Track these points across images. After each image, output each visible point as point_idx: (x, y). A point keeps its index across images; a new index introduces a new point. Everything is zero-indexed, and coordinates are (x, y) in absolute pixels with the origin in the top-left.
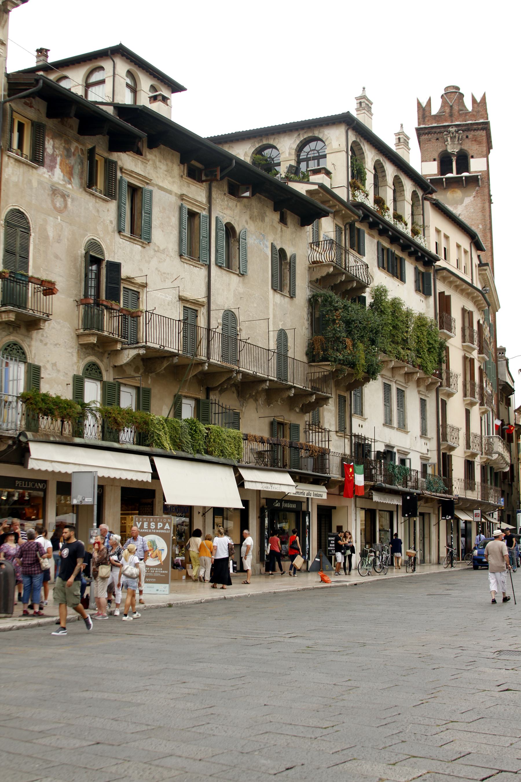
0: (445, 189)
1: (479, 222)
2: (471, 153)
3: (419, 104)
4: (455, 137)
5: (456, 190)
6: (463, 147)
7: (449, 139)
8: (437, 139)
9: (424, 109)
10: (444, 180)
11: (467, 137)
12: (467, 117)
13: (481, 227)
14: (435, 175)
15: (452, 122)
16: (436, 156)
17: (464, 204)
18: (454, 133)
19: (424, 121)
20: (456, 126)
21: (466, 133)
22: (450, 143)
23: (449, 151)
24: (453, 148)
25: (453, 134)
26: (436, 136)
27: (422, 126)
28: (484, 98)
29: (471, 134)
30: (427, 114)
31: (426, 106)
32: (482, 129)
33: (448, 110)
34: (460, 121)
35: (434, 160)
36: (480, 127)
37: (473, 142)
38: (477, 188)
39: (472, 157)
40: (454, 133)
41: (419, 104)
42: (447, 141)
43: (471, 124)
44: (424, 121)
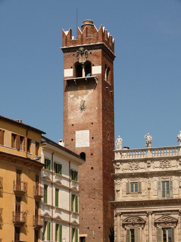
0: (77, 86)
1: (96, 105)
2: (93, 63)
5: (83, 86)
6: (88, 59)
8: (74, 55)
9: (66, 37)
10: (75, 80)
11: (91, 53)
12: (91, 41)
13: (97, 108)
14: (71, 77)
15: (82, 44)
16: (72, 65)
19: (66, 44)
20: (83, 46)
21: (90, 51)
22: (80, 57)
23: (80, 62)
24: (82, 60)
26: (73, 53)
27: (65, 47)
29: (93, 51)
30: (69, 39)
32: (100, 48)
33: (80, 37)
34: (87, 44)
35: (72, 68)
37: (94, 56)
39: (93, 65)
41: (64, 34)
44: (66, 44)
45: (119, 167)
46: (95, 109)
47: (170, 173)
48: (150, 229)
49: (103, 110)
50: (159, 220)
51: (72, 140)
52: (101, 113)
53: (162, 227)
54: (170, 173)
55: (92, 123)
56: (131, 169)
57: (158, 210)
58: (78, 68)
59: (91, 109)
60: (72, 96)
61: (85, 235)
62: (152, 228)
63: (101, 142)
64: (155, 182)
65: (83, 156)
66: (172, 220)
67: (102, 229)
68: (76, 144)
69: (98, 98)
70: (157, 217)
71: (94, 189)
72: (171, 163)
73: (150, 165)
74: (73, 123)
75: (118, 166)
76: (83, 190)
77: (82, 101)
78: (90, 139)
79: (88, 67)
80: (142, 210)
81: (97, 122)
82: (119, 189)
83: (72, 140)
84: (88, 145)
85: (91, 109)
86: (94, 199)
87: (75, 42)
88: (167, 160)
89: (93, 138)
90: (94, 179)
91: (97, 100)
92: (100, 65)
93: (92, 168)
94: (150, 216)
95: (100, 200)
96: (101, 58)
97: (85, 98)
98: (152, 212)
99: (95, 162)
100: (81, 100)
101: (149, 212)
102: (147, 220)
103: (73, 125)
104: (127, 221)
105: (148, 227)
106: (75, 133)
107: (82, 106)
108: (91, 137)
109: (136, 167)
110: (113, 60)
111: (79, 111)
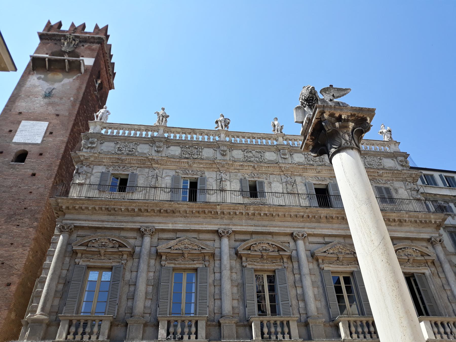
0: (48, 71)
3: (49, 22)
4: (72, 43)
5: (59, 73)
7: (66, 43)
8: (56, 44)
10: (47, 59)
13: (72, 99)
17: (62, 83)
18: (71, 39)
25: (70, 39)
26: (55, 42)
32: (98, 43)
36: (96, 41)
38: (79, 74)
40: (71, 39)
42: (64, 44)
43: (89, 37)
45: (94, 145)
46: (69, 99)
47: (201, 166)
48: (143, 266)
49: (82, 104)
52: (78, 105)
53: (173, 265)
54: (201, 166)
59: (61, 99)
62: (149, 266)
63: (66, 139)
64: (167, 178)
65: (22, 157)
66: (202, 248)
67: (13, 288)
69: (80, 88)
71: (25, 208)
72: (203, 152)
74: (21, 111)
75: (92, 143)
78: (46, 133)
80: (130, 224)
81: (67, 114)
84: (39, 141)
85: (61, 99)
87: (64, 31)
88: (196, 147)
91: (75, 92)
92: (93, 58)
94: (147, 240)
95: (31, 230)
96: (97, 52)
97: (56, 85)
99: (44, 171)
101: (146, 230)
103: (20, 113)
105: (136, 264)
106: (19, 123)
107: (47, 92)
108: (50, 130)
110: (110, 89)
111: (40, 98)
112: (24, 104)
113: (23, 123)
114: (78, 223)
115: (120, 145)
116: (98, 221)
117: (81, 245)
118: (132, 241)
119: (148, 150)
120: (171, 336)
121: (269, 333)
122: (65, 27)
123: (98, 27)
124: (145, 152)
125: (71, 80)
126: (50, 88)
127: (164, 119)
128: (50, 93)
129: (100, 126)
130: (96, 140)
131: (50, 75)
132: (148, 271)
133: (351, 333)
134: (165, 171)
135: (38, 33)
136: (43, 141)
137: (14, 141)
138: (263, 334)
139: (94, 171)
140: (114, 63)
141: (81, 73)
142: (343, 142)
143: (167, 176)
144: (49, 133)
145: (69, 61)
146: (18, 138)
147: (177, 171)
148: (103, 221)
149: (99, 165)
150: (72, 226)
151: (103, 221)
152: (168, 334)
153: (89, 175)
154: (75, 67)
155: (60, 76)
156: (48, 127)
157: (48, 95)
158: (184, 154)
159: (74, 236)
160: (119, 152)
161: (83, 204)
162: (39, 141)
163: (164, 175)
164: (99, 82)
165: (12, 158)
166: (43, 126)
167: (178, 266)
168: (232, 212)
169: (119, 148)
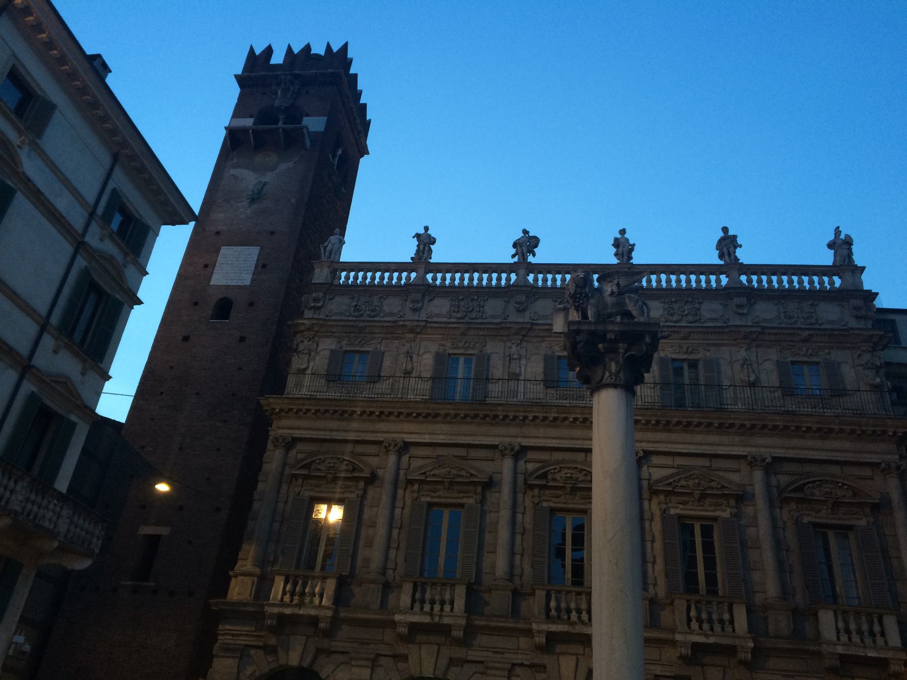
3: (252, 50)
8: (264, 94)
11: (307, 92)
13: (293, 201)
17: (277, 171)
28: (345, 47)
31: (260, 54)
35: (251, 117)
39: (308, 116)
41: (252, 50)
42: (276, 94)
45: (319, 305)
50: (424, 473)
51: (206, 266)
53: (428, 499)
54: (482, 333)
55: (272, 233)
56: (356, 314)
57: (427, 439)
58: (265, 117)
60: (232, 171)
61: (164, 531)
64: (427, 356)
66: (472, 474)
68: (214, 276)
70: (416, 463)
71: (233, 394)
73: (419, 305)
76: (197, 394)
77: (260, 182)
78: (256, 266)
79: (294, 115)
82: (303, 367)
83: (206, 266)
84: (248, 283)
86: (225, 421)
89: (264, 266)
90: (240, 369)
93: (242, 339)
97: (268, 177)
98: (402, 444)
100: (256, 181)
102: (380, 472)
103: (218, 233)
104: (307, 466)
106: (218, 251)
109: (372, 311)
111: (246, 203)
112: (221, 216)
113: (224, 250)
114: (298, 433)
115: (359, 300)
116: (325, 430)
117: (302, 467)
118: (374, 461)
119: (399, 308)
120: (417, 605)
121: (558, 609)
122: (278, 58)
123: (332, 51)
124: (396, 311)
125: (290, 164)
126: (260, 182)
127: (427, 249)
128: (260, 191)
129: (329, 267)
130: (321, 294)
131: (259, 159)
132: (393, 507)
133: (689, 620)
134: (423, 343)
135: (236, 76)
136: (252, 280)
137: (212, 283)
138: (548, 609)
139: (320, 348)
140: (365, 105)
141: (306, 149)
142: (607, 374)
143: (425, 353)
144: (262, 266)
145: (284, 130)
146: (218, 279)
147: (443, 343)
148: (331, 430)
149: (328, 337)
150: (290, 439)
151: (331, 430)
152: (414, 601)
153: (313, 354)
154: (292, 141)
155: (273, 158)
156: (259, 255)
157: (256, 197)
158: (454, 311)
159: (293, 453)
160: (356, 314)
161: (304, 404)
162: (248, 283)
163: (422, 351)
164: (340, 152)
165: (211, 312)
166: (250, 255)
167: (436, 500)
168: (521, 415)
169: (356, 306)
